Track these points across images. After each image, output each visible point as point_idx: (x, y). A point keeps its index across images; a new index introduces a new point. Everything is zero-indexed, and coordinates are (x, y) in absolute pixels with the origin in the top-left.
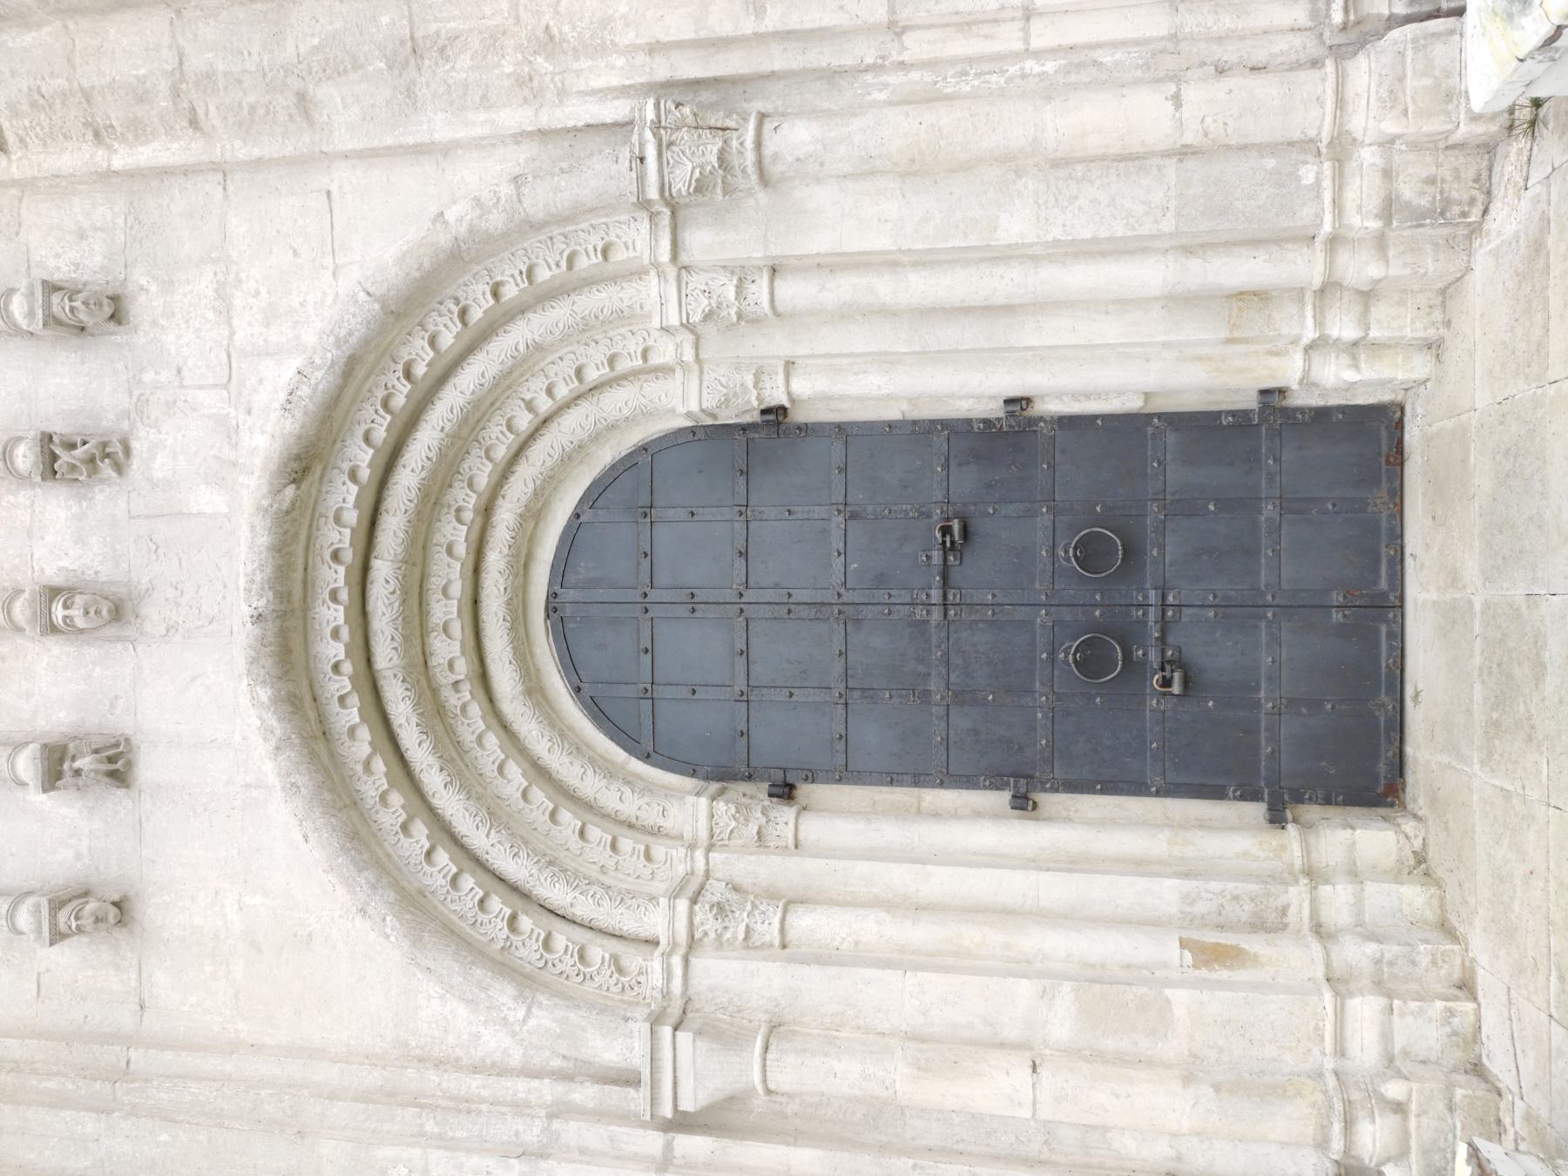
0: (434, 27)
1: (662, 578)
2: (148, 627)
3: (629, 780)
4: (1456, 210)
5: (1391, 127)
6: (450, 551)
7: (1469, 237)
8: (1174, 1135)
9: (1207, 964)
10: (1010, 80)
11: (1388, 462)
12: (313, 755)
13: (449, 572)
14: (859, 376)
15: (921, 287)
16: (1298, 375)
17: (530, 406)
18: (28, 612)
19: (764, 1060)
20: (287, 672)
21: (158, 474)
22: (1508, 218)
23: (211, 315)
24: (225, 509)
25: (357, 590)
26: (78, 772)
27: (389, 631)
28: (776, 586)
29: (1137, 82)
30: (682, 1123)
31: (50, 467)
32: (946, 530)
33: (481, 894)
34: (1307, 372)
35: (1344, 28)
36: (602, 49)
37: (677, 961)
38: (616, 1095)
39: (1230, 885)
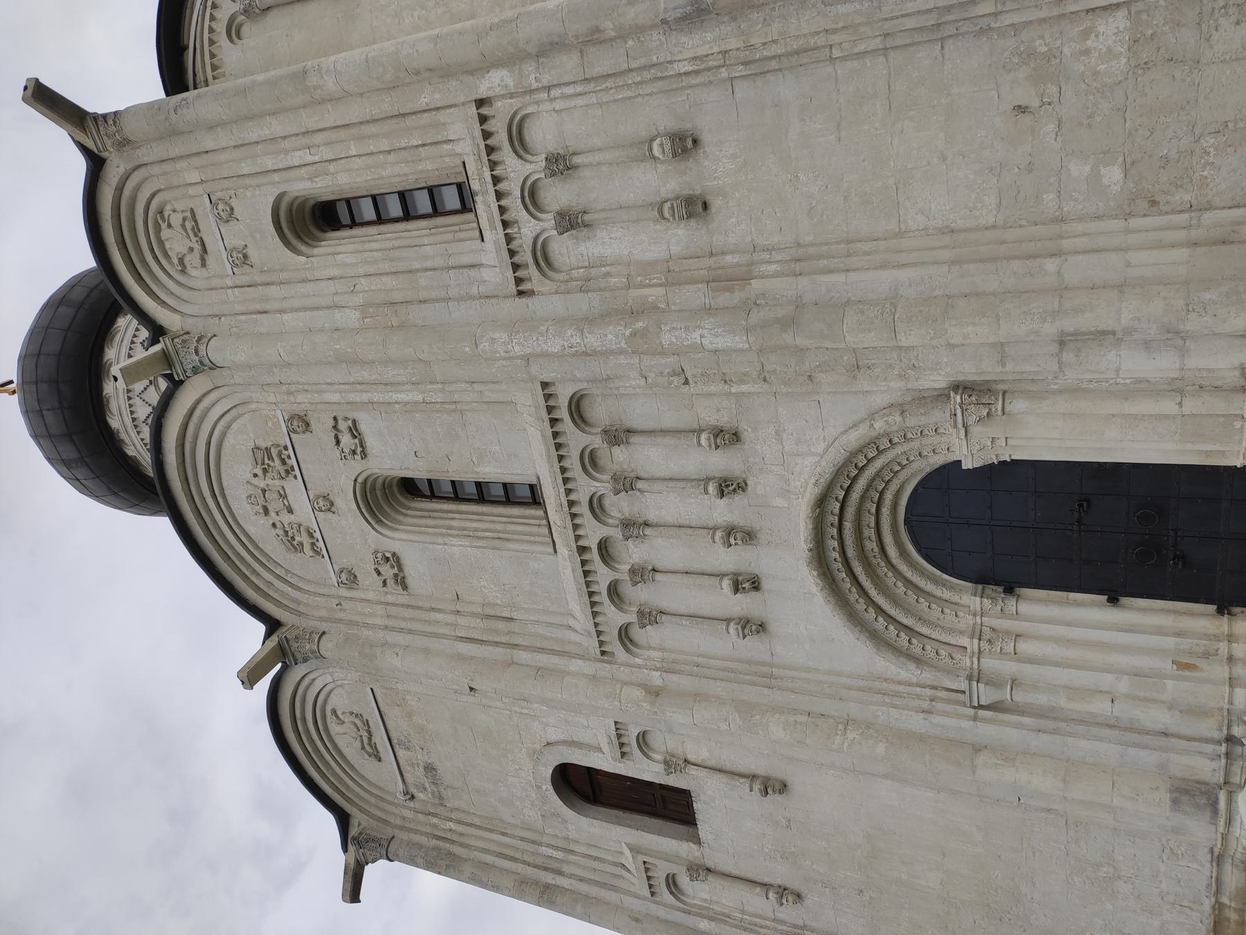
3: (943, 584)
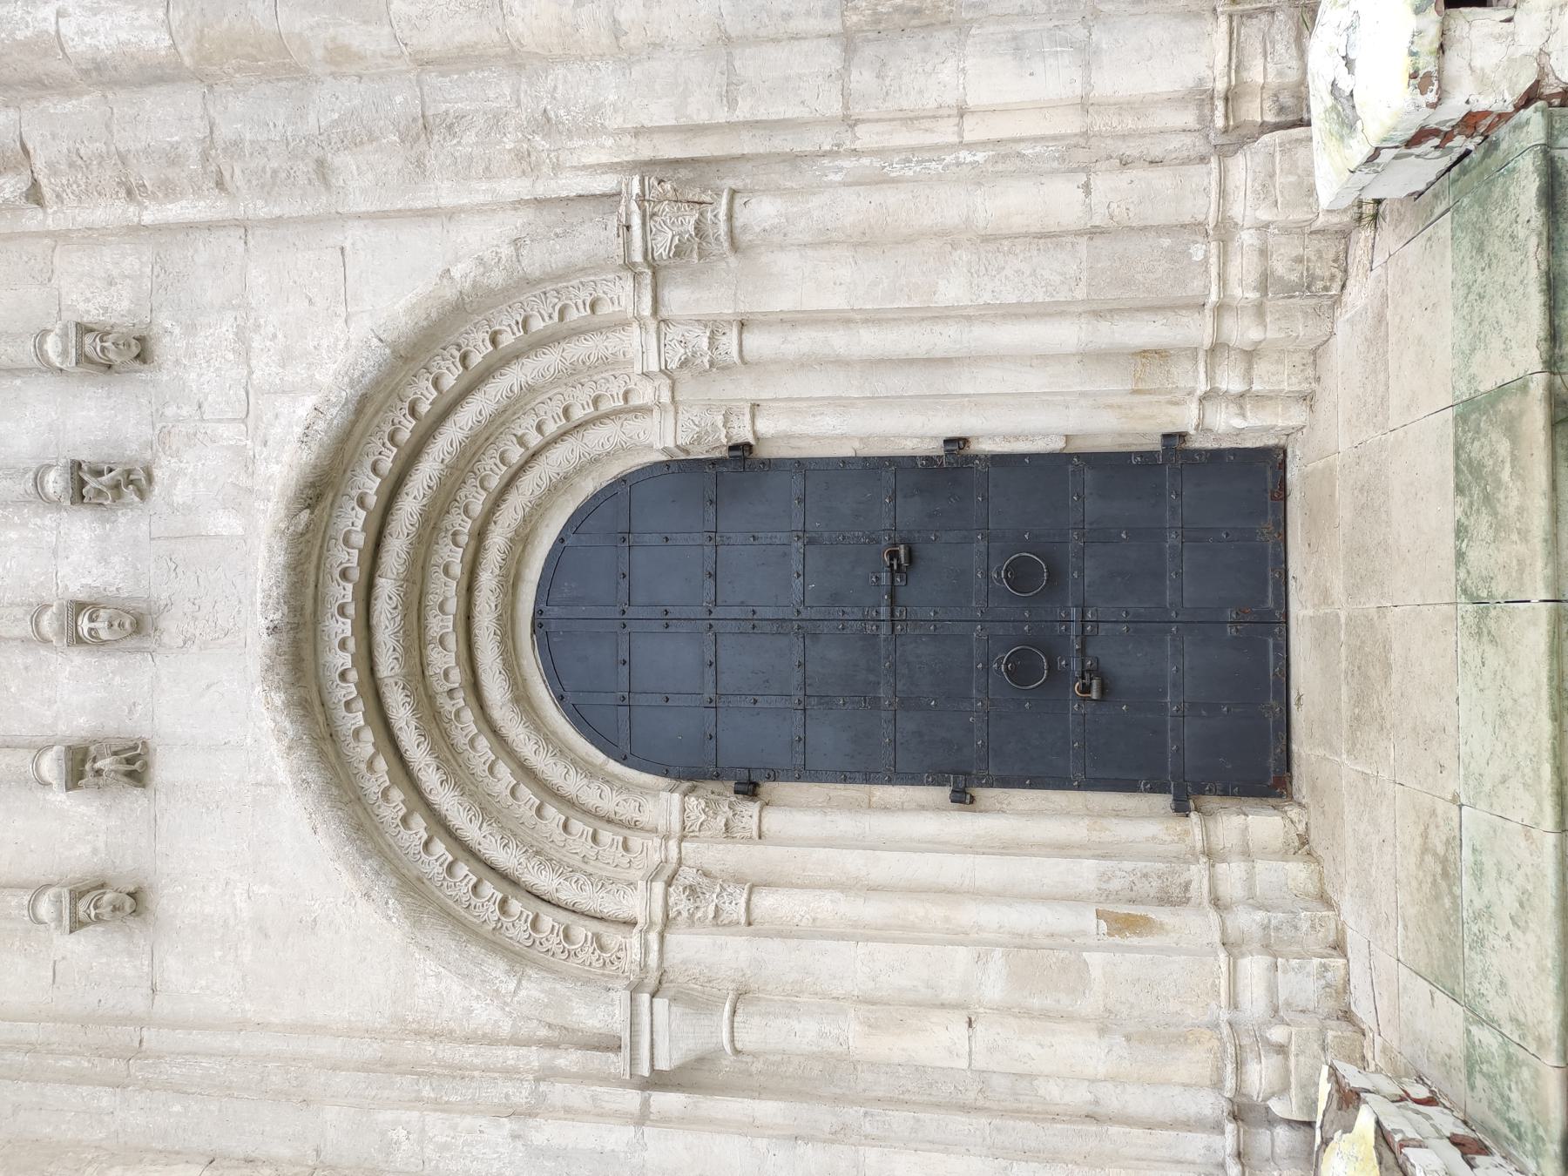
0: (444, 107)
1: (639, 597)
2: (166, 639)
3: (609, 779)
4: (1320, 284)
5: (1264, 215)
6: (446, 572)
7: (1332, 307)
8: (1093, 1081)
9: (1120, 931)
10: (947, 166)
11: (1273, 498)
12: (322, 754)
13: (446, 590)
14: (816, 418)
15: (870, 341)
16: (1195, 422)
17: (521, 441)
18: (56, 625)
19: (732, 1022)
20: (299, 679)
21: (178, 499)
22: (1359, 294)
23: (230, 356)
24: (240, 531)
25: (362, 605)
26: (98, 773)
27: (391, 643)
28: (742, 604)
29: (1054, 172)
30: (659, 1081)
31: (78, 492)
32: (894, 555)
33: (475, 879)
34: (1201, 418)
35: (1226, 131)
36: (595, 131)
37: (653, 937)
38: (597, 1060)
39: (1141, 864)
